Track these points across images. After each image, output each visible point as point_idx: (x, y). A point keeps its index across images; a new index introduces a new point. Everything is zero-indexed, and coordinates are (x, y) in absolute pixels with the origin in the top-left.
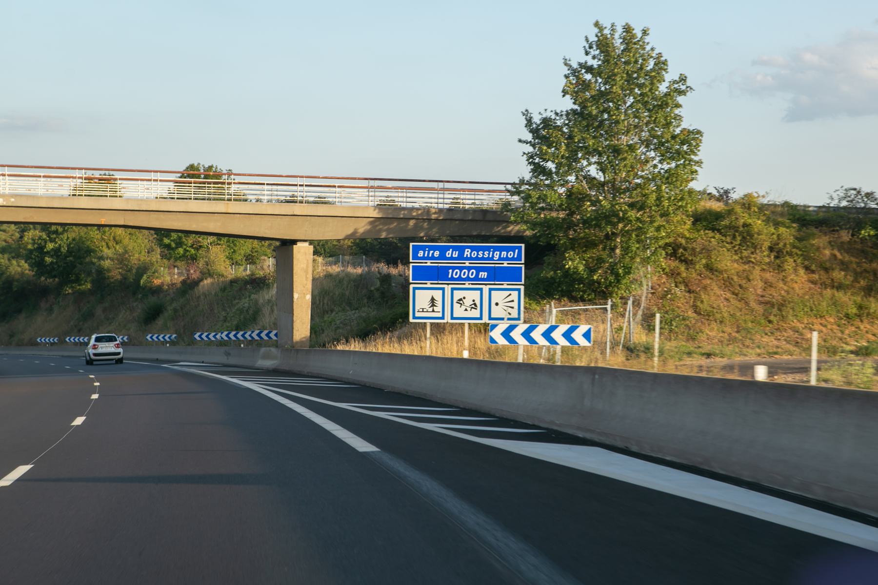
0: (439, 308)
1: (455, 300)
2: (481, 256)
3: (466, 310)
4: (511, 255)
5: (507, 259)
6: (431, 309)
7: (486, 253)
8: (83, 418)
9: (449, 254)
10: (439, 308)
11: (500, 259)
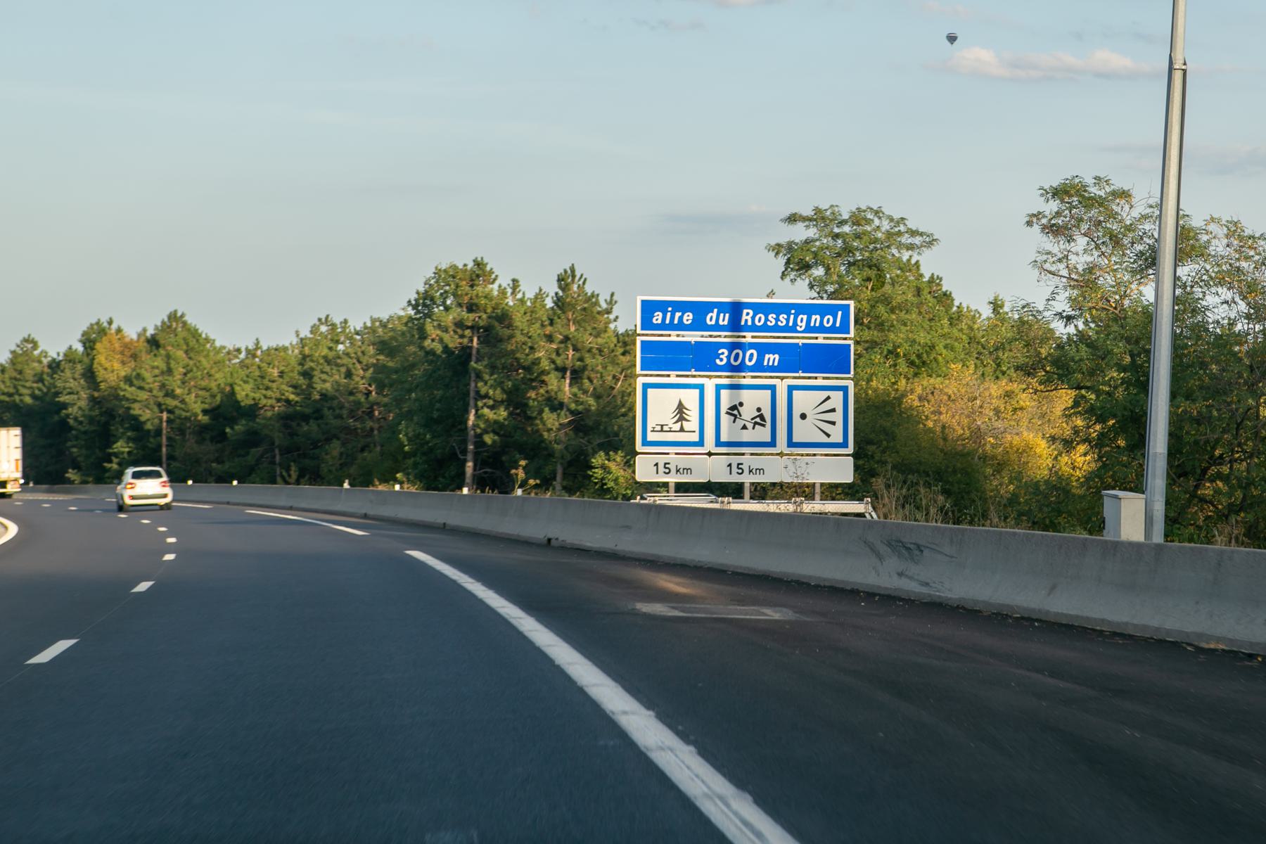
0: (692, 424)
1: (724, 408)
2: (772, 323)
3: (744, 427)
4: (828, 321)
5: (821, 329)
6: (677, 427)
7: (783, 317)
8: (150, 583)
9: (711, 319)
10: (692, 424)
11: (809, 329)
